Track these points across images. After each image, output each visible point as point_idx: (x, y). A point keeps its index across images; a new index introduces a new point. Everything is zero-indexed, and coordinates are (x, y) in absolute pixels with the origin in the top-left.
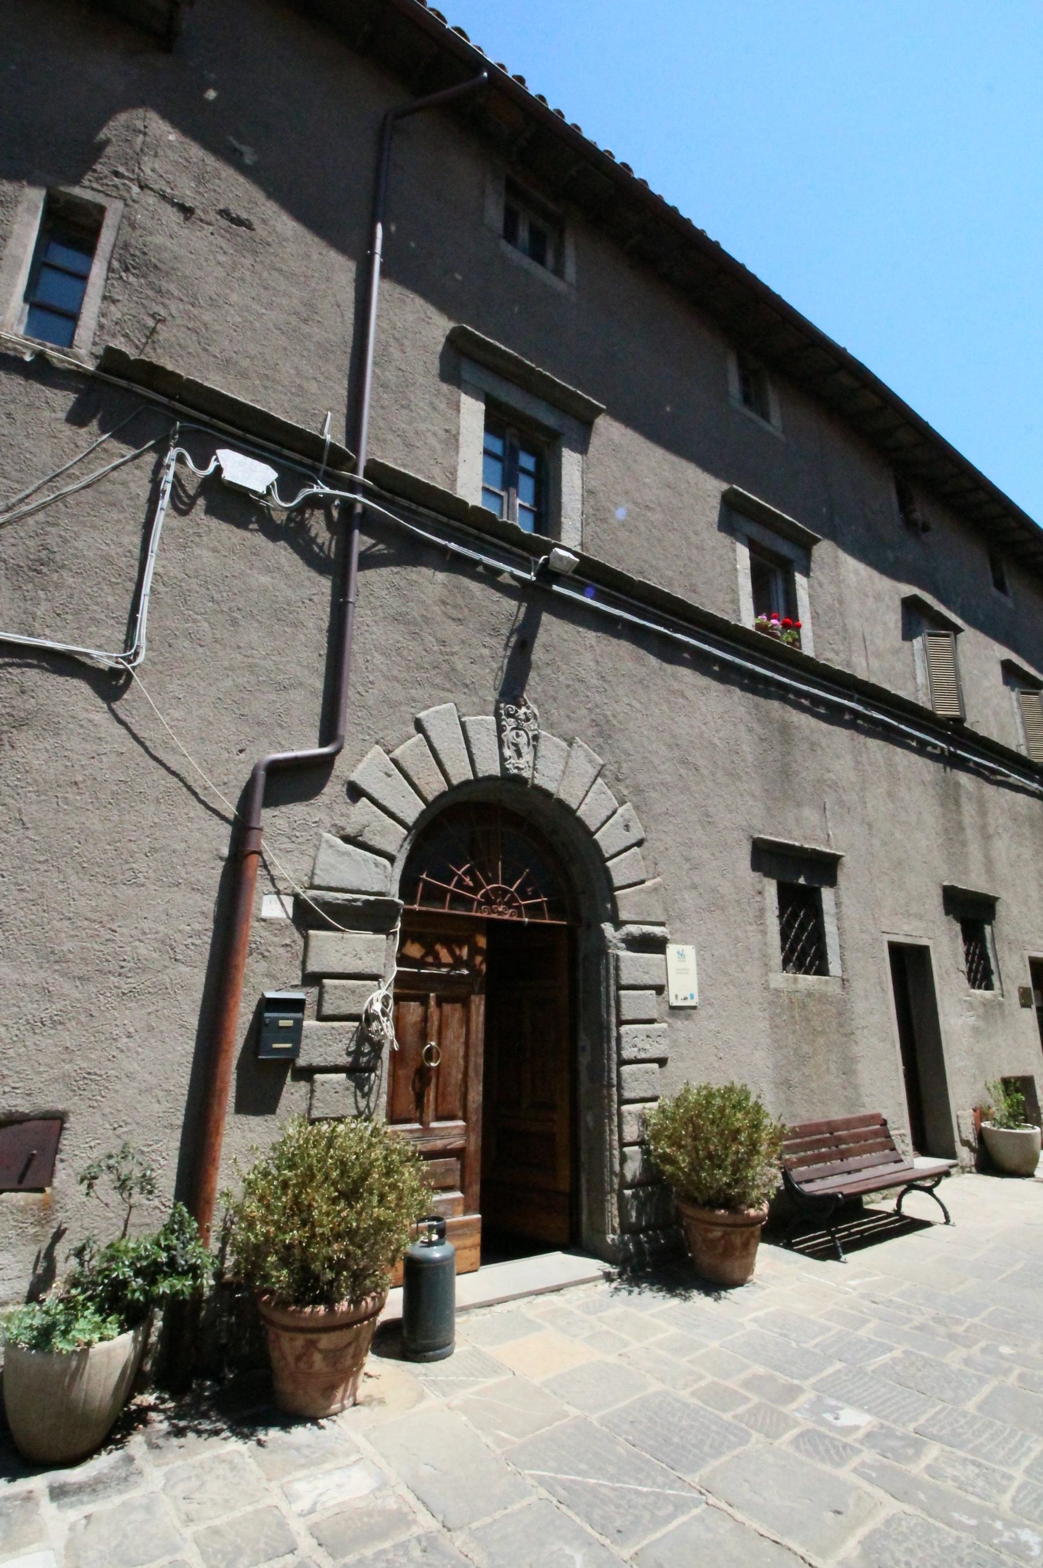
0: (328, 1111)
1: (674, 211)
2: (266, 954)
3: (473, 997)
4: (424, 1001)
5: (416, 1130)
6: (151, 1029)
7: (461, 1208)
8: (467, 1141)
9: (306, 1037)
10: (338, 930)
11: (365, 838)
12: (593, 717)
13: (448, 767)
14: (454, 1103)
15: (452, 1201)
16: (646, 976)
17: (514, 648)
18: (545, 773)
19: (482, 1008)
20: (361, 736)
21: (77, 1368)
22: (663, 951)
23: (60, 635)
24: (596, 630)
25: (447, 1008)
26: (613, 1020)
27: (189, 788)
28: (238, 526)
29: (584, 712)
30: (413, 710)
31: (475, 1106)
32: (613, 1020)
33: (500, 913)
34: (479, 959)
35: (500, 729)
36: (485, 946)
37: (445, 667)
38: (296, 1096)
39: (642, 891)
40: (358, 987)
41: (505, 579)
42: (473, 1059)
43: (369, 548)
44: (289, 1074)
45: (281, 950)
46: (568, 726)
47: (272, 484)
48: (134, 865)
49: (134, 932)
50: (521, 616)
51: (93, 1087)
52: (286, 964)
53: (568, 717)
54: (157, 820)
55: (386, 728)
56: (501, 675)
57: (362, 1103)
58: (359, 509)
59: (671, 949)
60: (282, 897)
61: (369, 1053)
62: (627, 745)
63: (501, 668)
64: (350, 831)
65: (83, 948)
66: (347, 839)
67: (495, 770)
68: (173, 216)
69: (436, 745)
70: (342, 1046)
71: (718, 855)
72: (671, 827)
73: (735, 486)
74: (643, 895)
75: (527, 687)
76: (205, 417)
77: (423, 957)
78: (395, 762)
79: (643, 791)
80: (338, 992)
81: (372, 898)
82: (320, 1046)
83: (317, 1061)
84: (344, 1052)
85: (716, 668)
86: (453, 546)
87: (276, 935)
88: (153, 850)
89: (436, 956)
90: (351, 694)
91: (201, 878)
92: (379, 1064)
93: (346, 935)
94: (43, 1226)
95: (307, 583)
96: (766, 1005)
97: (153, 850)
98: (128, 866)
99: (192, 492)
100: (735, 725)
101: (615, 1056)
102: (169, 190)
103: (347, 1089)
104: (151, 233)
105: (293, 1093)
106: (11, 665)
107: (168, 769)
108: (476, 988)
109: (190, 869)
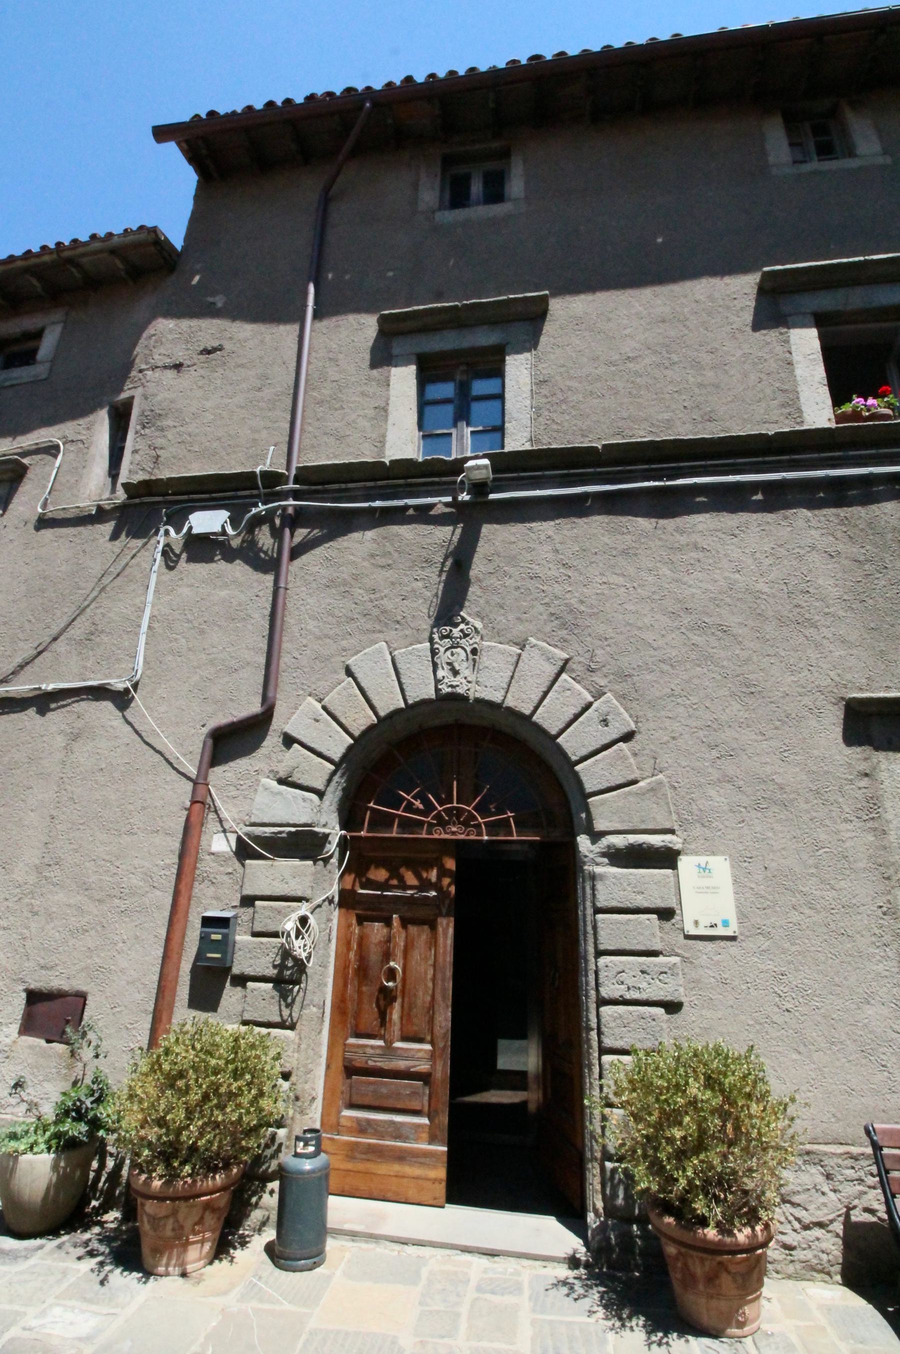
0: (256, 1015)
1: (608, 51)
2: (214, 881)
3: (439, 920)
4: (388, 922)
5: (379, 1047)
6: (137, 937)
7: (425, 1136)
8: (433, 1066)
9: (240, 949)
10: (270, 859)
11: (296, 778)
12: (552, 610)
13: (376, 703)
14: (419, 1024)
15: (418, 1126)
16: (639, 897)
17: (449, 573)
18: (487, 684)
19: (451, 931)
20: (295, 693)
21: (13, 1169)
22: (673, 866)
23: (99, 676)
24: (552, 519)
25: (413, 929)
26: (591, 950)
27: (167, 760)
28: (207, 562)
29: (542, 608)
30: (343, 659)
31: (442, 1031)
32: (591, 950)
33: (454, 833)
34: (446, 881)
35: (434, 652)
36: (454, 868)
37: (376, 612)
38: (234, 999)
39: (630, 793)
40: (284, 907)
41: (440, 510)
42: (440, 982)
43: (306, 537)
44: (229, 980)
45: (226, 878)
46: (519, 630)
47: (226, 522)
48: (132, 821)
49: (129, 868)
50: (456, 539)
51: (102, 976)
52: (229, 889)
53: (519, 619)
54: (146, 787)
55: (318, 679)
56: (436, 601)
57: (286, 1012)
58: (290, 511)
59: (685, 863)
60: (228, 834)
61: (292, 967)
62: (601, 629)
63: (436, 595)
64: (282, 774)
65: (100, 880)
66: (282, 781)
67: (430, 693)
68: (171, 374)
69: (363, 684)
70: (269, 959)
71: (769, 734)
72: (681, 710)
73: (766, 269)
74: (631, 799)
75: (467, 604)
76: (185, 497)
77: (387, 880)
78: (324, 708)
79: (630, 676)
80: (267, 913)
81: (293, 829)
82: (251, 958)
83: (249, 971)
84: (271, 965)
85: (759, 497)
86: (378, 504)
87: (222, 866)
88: (144, 808)
89: (401, 879)
90: (285, 660)
91: (172, 825)
92: (304, 977)
93: (275, 863)
94: (69, 1069)
95: (255, 584)
96: (887, 938)
97: (144, 808)
98: (127, 821)
99: (178, 551)
100: (800, 557)
101: (593, 993)
102: (169, 360)
103: (273, 998)
104: (156, 395)
105: (231, 996)
106: (73, 702)
107: (154, 749)
108: (444, 911)
109: (165, 819)
